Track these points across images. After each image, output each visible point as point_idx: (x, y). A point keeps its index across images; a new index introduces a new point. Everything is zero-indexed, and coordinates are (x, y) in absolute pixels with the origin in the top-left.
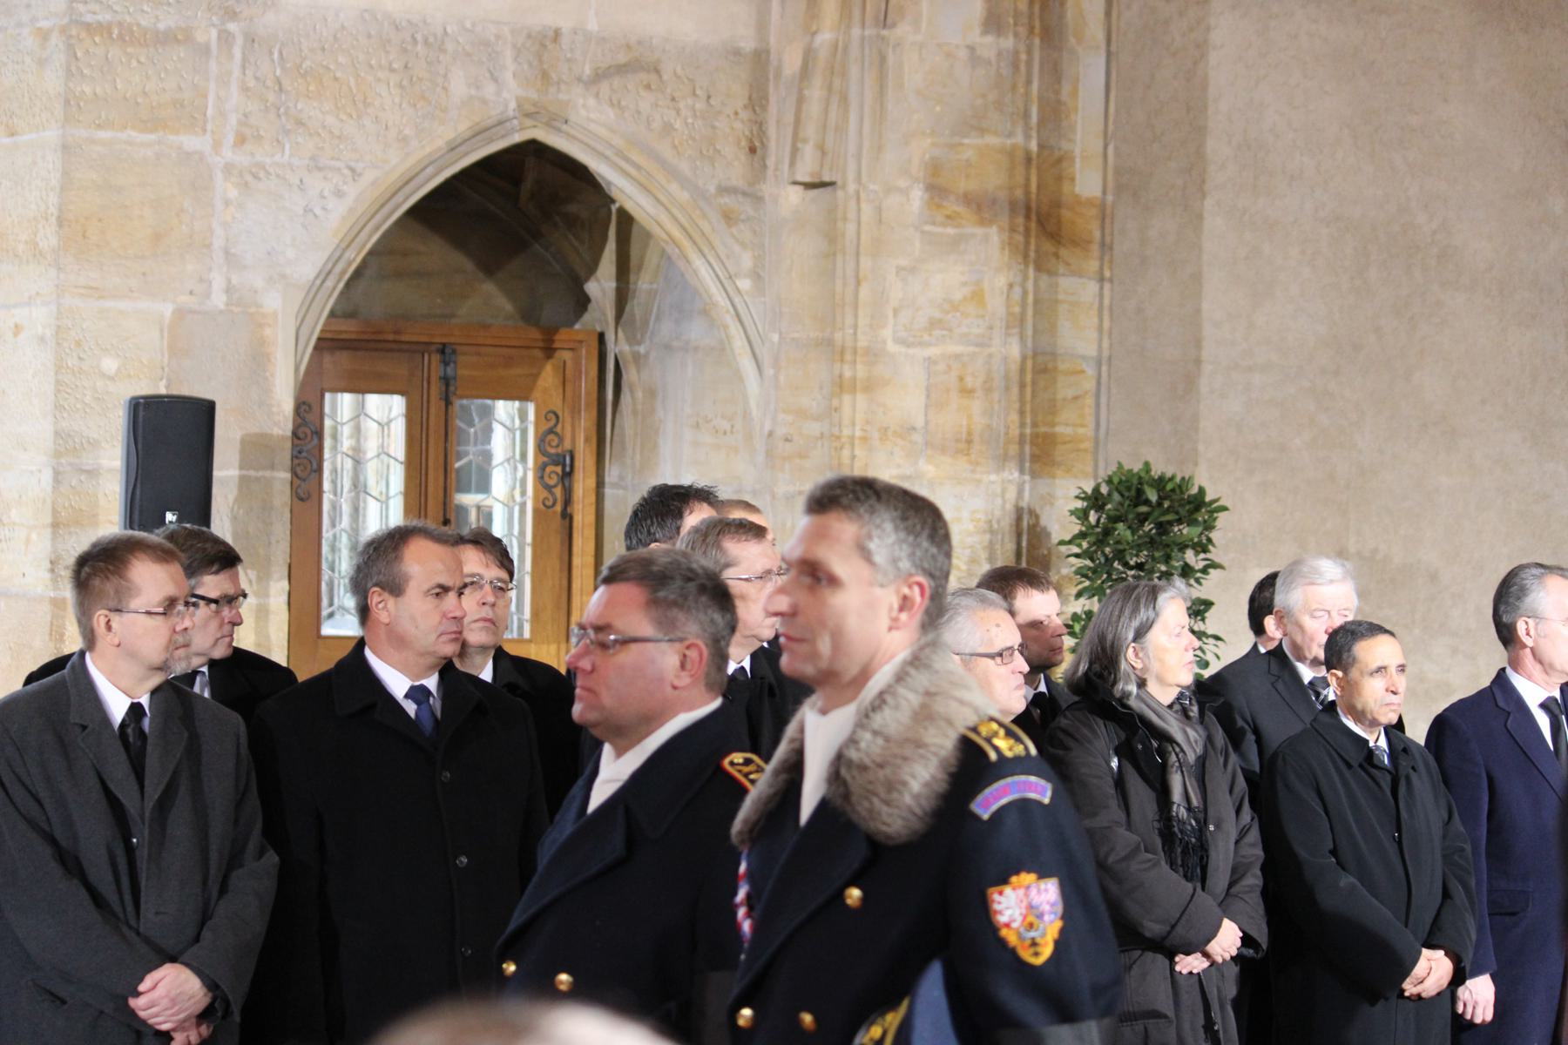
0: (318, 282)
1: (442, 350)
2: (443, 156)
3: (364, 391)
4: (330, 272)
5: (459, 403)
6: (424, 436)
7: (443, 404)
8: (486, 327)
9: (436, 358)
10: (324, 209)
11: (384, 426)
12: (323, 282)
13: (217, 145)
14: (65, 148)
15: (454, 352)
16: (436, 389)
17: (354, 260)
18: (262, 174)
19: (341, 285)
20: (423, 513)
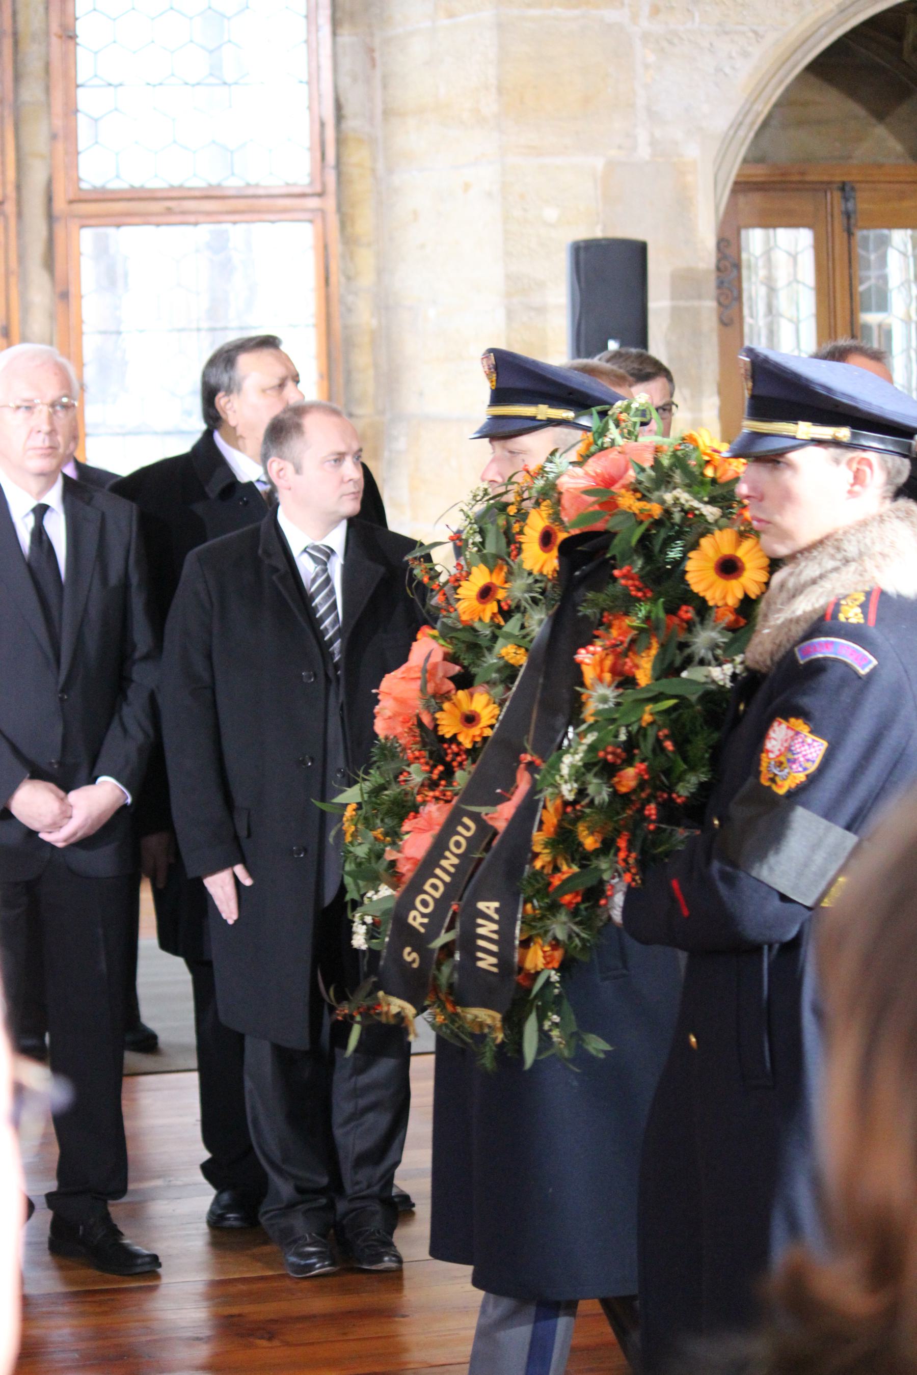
0: (731, 133)
1: (843, 187)
2: (834, 17)
3: (775, 226)
4: (741, 124)
5: (859, 234)
6: (831, 265)
7: (845, 235)
8: (880, 166)
9: (837, 195)
10: (733, 68)
11: (794, 257)
12: (736, 132)
13: (634, 18)
14: (501, 26)
15: (853, 189)
16: (839, 222)
17: (762, 111)
18: (676, 41)
19: (752, 135)
20: (833, 335)
